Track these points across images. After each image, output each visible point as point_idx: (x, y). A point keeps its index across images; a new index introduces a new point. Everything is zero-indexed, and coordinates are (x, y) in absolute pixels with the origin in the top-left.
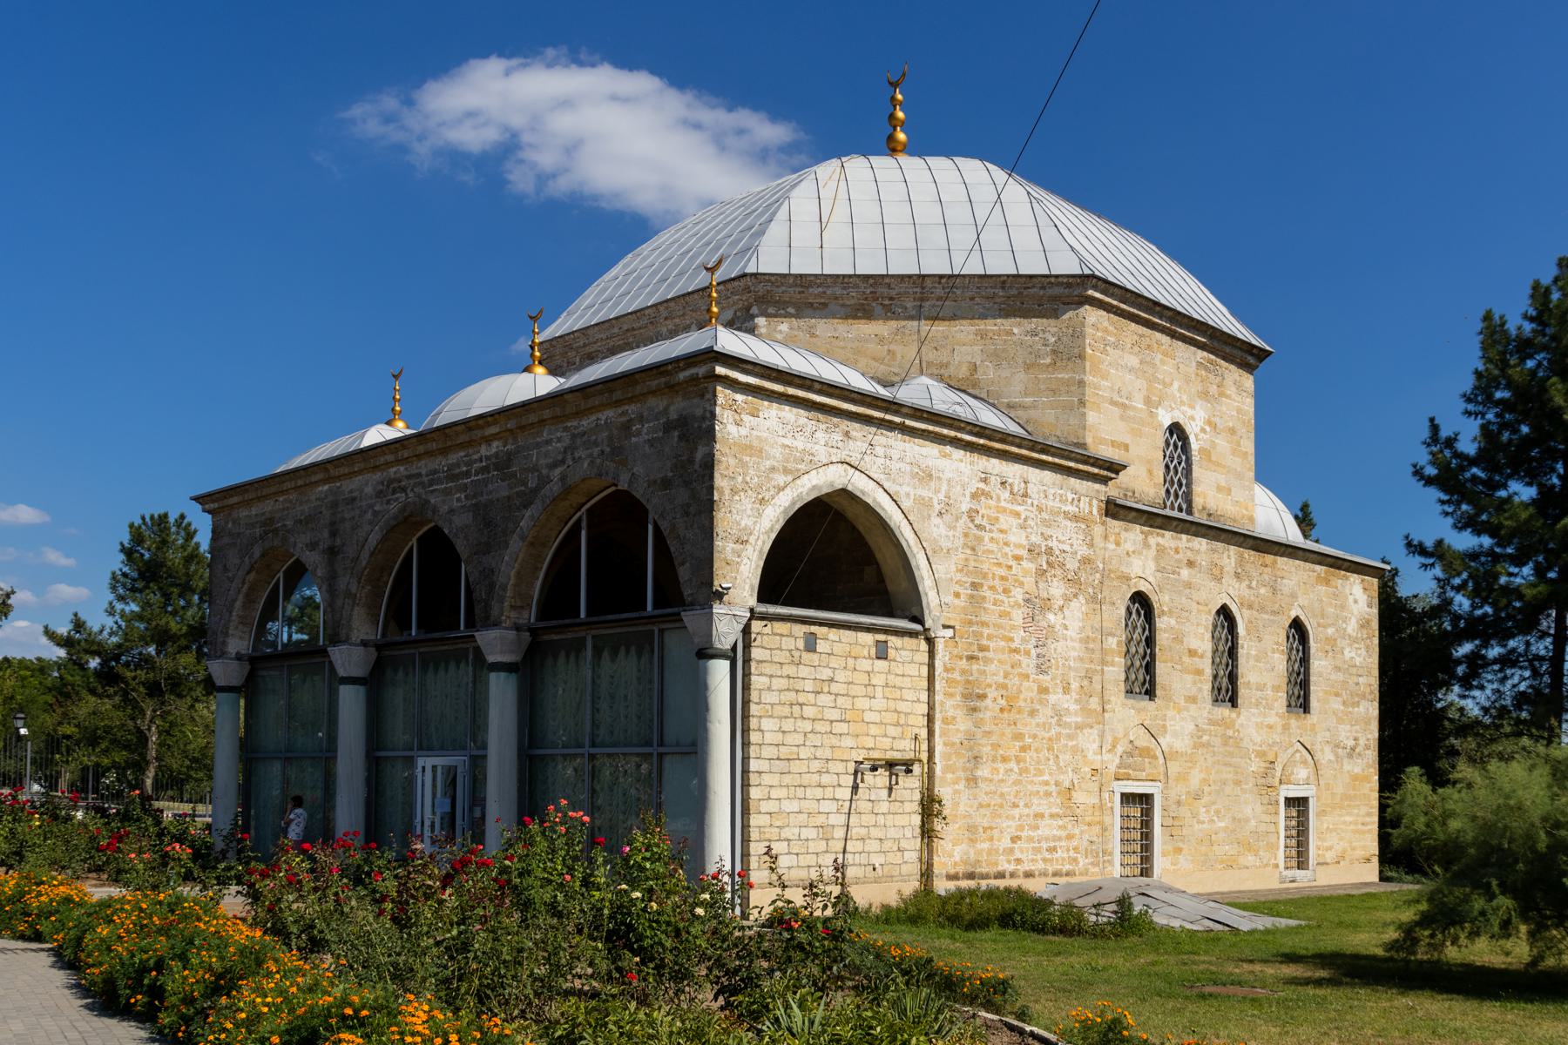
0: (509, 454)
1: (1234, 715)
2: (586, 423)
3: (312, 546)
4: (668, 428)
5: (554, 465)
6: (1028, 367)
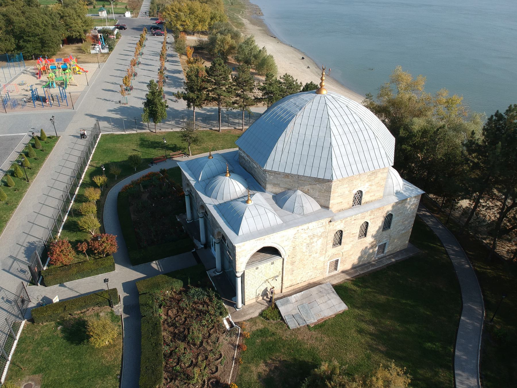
1: (365, 239)
6: (319, 192)
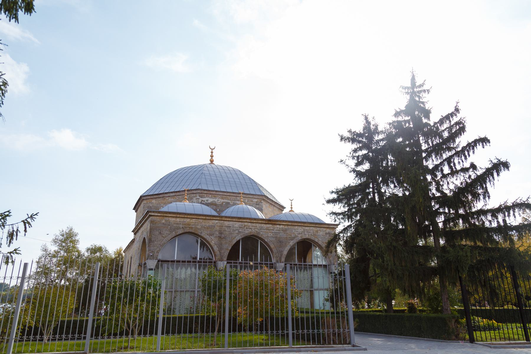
0: (286, 229)
2: (307, 228)
3: (211, 235)
4: (326, 234)
5: (299, 234)
